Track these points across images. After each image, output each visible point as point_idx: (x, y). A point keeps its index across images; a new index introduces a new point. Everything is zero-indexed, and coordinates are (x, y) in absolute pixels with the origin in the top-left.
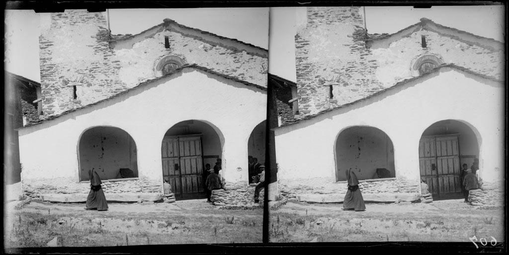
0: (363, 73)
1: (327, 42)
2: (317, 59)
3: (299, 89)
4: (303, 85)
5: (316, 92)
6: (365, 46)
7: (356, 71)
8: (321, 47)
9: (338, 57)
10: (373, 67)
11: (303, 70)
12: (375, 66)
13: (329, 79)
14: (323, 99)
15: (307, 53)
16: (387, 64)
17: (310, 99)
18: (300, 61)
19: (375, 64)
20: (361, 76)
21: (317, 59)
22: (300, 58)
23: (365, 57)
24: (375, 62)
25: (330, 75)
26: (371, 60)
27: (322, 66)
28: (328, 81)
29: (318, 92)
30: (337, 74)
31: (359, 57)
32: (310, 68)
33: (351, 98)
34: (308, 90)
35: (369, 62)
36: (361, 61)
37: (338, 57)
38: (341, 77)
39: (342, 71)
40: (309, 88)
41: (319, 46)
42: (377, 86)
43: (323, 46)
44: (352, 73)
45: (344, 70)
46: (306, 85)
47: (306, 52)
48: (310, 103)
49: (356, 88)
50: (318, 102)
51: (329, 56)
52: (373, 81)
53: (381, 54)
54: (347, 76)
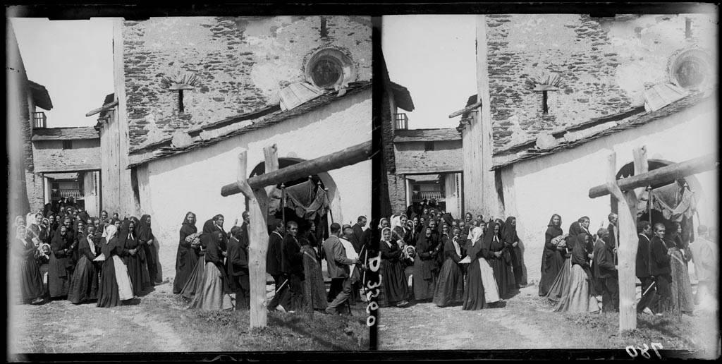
7: (220, 69)
10: (247, 64)
23: (235, 46)
35: (241, 55)
42: (253, 94)
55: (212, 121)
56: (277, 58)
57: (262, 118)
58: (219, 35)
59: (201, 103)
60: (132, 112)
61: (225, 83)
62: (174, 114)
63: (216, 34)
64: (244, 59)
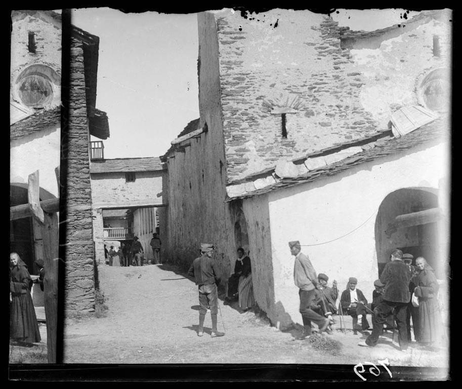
0: (340, 94)
1: (278, 37)
2: (259, 65)
4: (234, 112)
5: (258, 125)
6: (340, 47)
8: (266, 44)
9: (295, 64)
10: (355, 85)
12: (358, 83)
15: (240, 55)
16: (378, 80)
17: (247, 139)
18: (230, 68)
19: (358, 80)
20: (334, 99)
21: (259, 65)
22: (229, 62)
23: (341, 66)
24: (358, 76)
25: (282, 95)
26: (351, 72)
27: (267, 78)
29: (261, 126)
30: (295, 95)
31: (332, 66)
32: (246, 81)
33: (318, 137)
34: (243, 121)
36: (336, 73)
37: (295, 64)
38: (302, 99)
39: (302, 90)
40: (245, 117)
41: (262, 43)
42: (362, 119)
43: (270, 43)
44: (320, 93)
45: (306, 89)
46: (240, 112)
48: (247, 144)
49: (326, 120)
50: (260, 143)
51: (279, 62)
52: (355, 109)
53: (369, 63)
54: (311, 99)
55: (318, 149)
56: (387, 79)
57: (372, 144)
61: (331, 106)
62: (276, 141)
63: (320, 53)
64: (351, 80)
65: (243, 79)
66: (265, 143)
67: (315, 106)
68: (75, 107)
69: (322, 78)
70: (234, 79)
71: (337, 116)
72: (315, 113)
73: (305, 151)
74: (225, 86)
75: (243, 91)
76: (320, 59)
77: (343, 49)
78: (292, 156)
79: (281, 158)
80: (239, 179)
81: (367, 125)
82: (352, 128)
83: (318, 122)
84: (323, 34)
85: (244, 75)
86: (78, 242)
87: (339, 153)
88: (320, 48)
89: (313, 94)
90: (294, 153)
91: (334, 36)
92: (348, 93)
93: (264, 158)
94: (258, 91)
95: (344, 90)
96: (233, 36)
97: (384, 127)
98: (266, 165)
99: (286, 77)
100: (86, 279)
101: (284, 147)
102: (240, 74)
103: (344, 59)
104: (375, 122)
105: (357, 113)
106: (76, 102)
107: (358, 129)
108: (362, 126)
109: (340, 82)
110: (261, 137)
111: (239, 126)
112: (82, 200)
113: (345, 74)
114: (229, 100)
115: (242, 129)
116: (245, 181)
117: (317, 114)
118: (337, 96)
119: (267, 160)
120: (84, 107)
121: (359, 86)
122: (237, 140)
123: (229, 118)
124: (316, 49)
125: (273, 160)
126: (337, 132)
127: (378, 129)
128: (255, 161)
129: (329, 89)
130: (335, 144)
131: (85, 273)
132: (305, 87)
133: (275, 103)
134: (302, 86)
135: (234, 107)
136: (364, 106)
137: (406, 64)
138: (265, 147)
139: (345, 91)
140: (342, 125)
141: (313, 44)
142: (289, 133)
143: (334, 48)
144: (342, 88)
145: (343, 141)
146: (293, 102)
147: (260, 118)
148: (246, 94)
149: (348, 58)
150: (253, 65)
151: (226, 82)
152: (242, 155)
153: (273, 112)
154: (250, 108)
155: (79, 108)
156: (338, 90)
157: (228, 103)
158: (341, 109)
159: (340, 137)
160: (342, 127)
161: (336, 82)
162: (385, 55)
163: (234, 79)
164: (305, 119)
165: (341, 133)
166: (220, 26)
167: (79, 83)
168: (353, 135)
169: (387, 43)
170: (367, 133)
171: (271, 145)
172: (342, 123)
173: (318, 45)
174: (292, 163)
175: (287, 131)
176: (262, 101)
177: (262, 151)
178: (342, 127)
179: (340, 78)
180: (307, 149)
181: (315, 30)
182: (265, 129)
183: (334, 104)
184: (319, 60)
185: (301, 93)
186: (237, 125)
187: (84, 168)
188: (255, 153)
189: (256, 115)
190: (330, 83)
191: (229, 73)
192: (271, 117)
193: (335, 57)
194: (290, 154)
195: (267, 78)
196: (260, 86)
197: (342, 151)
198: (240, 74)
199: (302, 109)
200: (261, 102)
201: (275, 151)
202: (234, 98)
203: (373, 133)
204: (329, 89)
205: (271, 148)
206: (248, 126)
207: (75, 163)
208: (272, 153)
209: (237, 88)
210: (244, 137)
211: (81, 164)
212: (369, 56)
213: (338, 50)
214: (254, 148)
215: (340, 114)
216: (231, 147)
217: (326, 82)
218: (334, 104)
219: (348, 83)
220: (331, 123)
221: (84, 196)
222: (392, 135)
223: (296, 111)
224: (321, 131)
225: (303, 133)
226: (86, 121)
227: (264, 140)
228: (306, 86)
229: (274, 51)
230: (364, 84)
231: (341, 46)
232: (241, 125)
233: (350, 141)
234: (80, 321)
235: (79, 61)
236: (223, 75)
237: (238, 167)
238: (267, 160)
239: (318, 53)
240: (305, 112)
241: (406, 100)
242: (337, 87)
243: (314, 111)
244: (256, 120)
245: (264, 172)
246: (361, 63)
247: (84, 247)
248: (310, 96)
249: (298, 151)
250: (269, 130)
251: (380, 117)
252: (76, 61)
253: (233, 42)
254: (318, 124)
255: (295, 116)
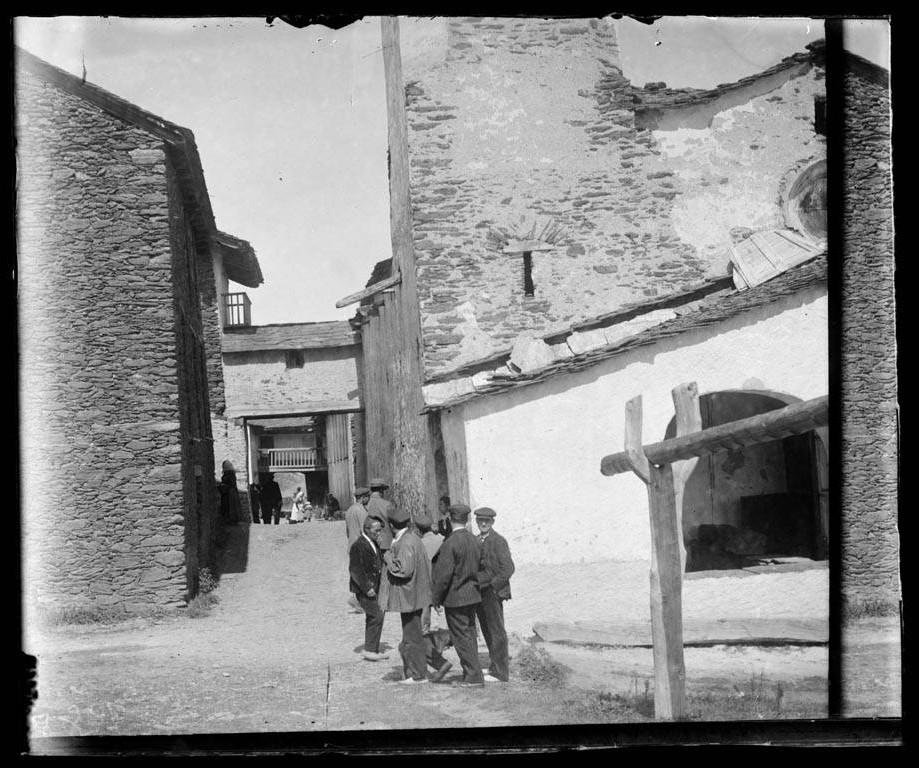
1: (516, 112)
2: (481, 165)
3: (423, 263)
4: (436, 252)
5: (480, 274)
6: (633, 126)
7: (607, 209)
10: (662, 195)
11: (436, 201)
12: (667, 191)
13: (522, 232)
14: (503, 297)
18: (428, 173)
19: (668, 186)
20: (622, 222)
21: (481, 165)
22: (426, 162)
23: (636, 161)
24: (667, 180)
26: (655, 172)
27: (495, 189)
28: (518, 239)
30: (546, 218)
34: (453, 267)
35: (650, 177)
40: (454, 261)
42: (677, 257)
43: (501, 124)
44: (596, 213)
46: (447, 251)
47: (444, 142)
48: (459, 309)
49: (606, 261)
50: (487, 307)
51: (518, 159)
52: (662, 239)
53: (688, 153)
55: (592, 314)
56: (724, 181)
57: (695, 305)
58: (604, 140)
59: (568, 279)
60: (429, 300)
61: (616, 235)
62: (513, 302)
63: (595, 138)
64: (656, 185)
65: (453, 192)
66: (494, 307)
67: (586, 237)
68: (151, 253)
69: (598, 185)
70: (436, 192)
71: (628, 254)
72: (586, 249)
73: (567, 319)
74: (420, 205)
75: (453, 213)
76: (595, 150)
77: (640, 130)
78: (543, 328)
79: (525, 332)
80: (445, 372)
81: (687, 268)
82: (657, 275)
83: (591, 266)
84: (601, 104)
85: (453, 183)
86: (158, 487)
87: (632, 321)
88: (594, 129)
89: (583, 214)
90: (547, 322)
91: (621, 105)
92: (650, 211)
93: (492, 333)
94: (480, 212)
95: (643, 204)
96: (433, 114)
97: (718, 271)
98: (495, 346)
99: (533, 185)
100: (173, 551)
101: (528, 313)
102: (447, 183)
103: (641, 148)
104: (701, 262)
105: (667, 246)
106: (154, 244)
107: (668, 277)
108: (675, 270)
109: (636, 191)
110: (486, 296)
111: (444, 276)
112: (164, 413)
113: (643, 176)
114: (427, 230)
115: (451, 282)
116: (456, 374)
117: (590, 251)
118: (627, 217)
119: (497, 337)
120: (168, 252)
121: (671, 197)
122: (442, 302)
123: (427, 263)
124: (588, 131)
125: (507, 337)
126: (628, 283)
127: (707, 275)
128: (474, 339)
129: (613, 204)
130: (626, 305)
131: (170, 540)
132: (566, 203)
133: (510, 232)
134: (561, 201)
135: (435, 242)
136: (680, 235)
137: (762, 152)
138: (494, 314)
139: (643, 206)
140: (637, 270)
141: (581, 123)
142: (538, 288)
143: (623, 128)
144: (639, 201)
145: (639, 298)
146: (545, 229)
147: (483, 261)
148: (457, 219)
149: (649, 146)
150: (469, 165)
151: (422, 199)
152: (450, 329)
153: (507, 249)
154: (465, 244)
155: (158, 254)
156: (629, 205)
157: (426, 235)
158: (636, 240)
159: (633, 293)
160: (637, 274)
161: (626, 191)
162: (719, 136)
163: (436, 192)
164: (567, 260)
165: (636, 285)
166: (410, 96)
167: (157, 210)
168: (659, 287)
169: (726, 117)
170: (687, 283)
171: (503, 310)
172: (639, 264)
173: (592, 125)
174: (542, 342)
175: (534, 283)
176: (487, 230)
177: (485, 319)
178: (637, 274)
179: (635, 183)
180: (572, 316)
181: (586, 97)
182: (493, 280)
183: (622, 233)
184: (592, 152)
185: (560, 214)
186: (442, 274)
187: (166, 358)
188: (475, 324)
189: (476, 257)
190: (615, 193)
191: (426, 181)
192: (504, 259)
193: (623, 145)
194: (539, 325)
195: (495, 189)
196: (483, 202)
197: (639, 318)
198: (447, 183)
199: (561, 242)
200: (484, 231)
201: (511, 320)
202: (435, 225)
203: (696, 283)
204: (613, 204)
205: (504, 315)
206: (462, 276)
207: (152, 350)
208: (506, 325)
209: (442, 208)
210: (453, 296)
211: (162, 351)
212: (689, 141)
213: (630, 132)
214: (473, 316)
215: (632, 250)
216: (430, 315)
217: (607, 191)
218: (622, 233)
219: (649, 192)
220: (616, 267)
221: (167, 407)
222: (734, 287)
223: (551, 247)
224: (596, 281)
225: (563, 286)
226: (170, 276)
227: (492, 300)
228: (569, 200)
229: (509, 139)
230: (680, 194)
231: (636, 124)
232: (449, 275)
233: (652, 299)
234: (160, 622)
235: (158, 173)
236: (417, 186)
237: (445, 350)
238: (497, 337)
239: (591, 139)
240: (566, 248)
241: (761, 220)
242: (627, 200)
243: (584, 245)
244: (476, 265)
245: (492, 358)
246: (672, 154)
247: (167, 494)
248: (577, 218)
249: (553, 320)
250: (501, 282)
251: (711, 253)
252: (153, 173)
253: (433, 126)
254: (592, 270)
255: (547, 255)
